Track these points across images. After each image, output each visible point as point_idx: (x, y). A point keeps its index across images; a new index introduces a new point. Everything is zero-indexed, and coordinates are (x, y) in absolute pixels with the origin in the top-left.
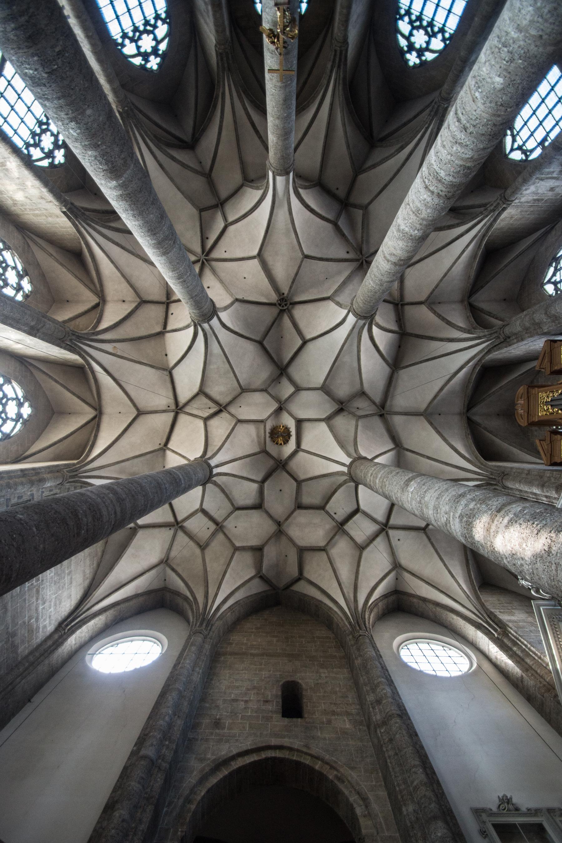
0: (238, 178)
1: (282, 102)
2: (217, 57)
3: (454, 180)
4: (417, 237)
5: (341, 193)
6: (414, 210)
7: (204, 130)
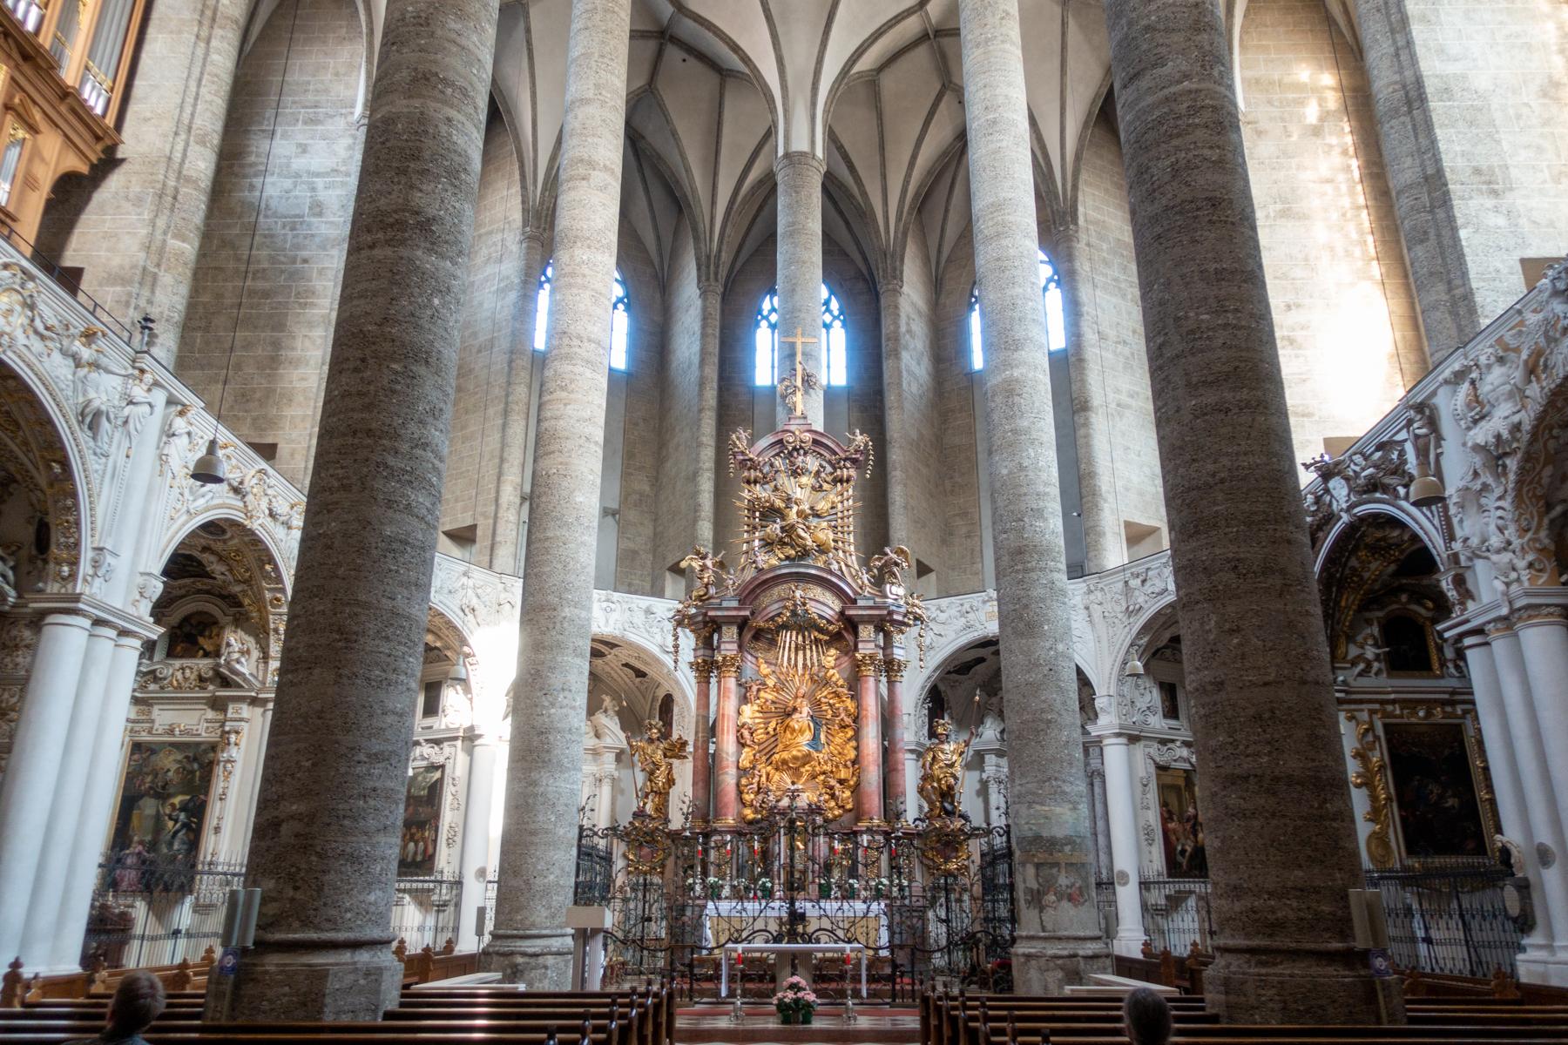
0: (888, 82)
1: (798, 289)
2: (902, 273)
3: (570, 367)
4: (579, 244)
5: (673, 54)
6: (602, 299)
7: (944, 154)
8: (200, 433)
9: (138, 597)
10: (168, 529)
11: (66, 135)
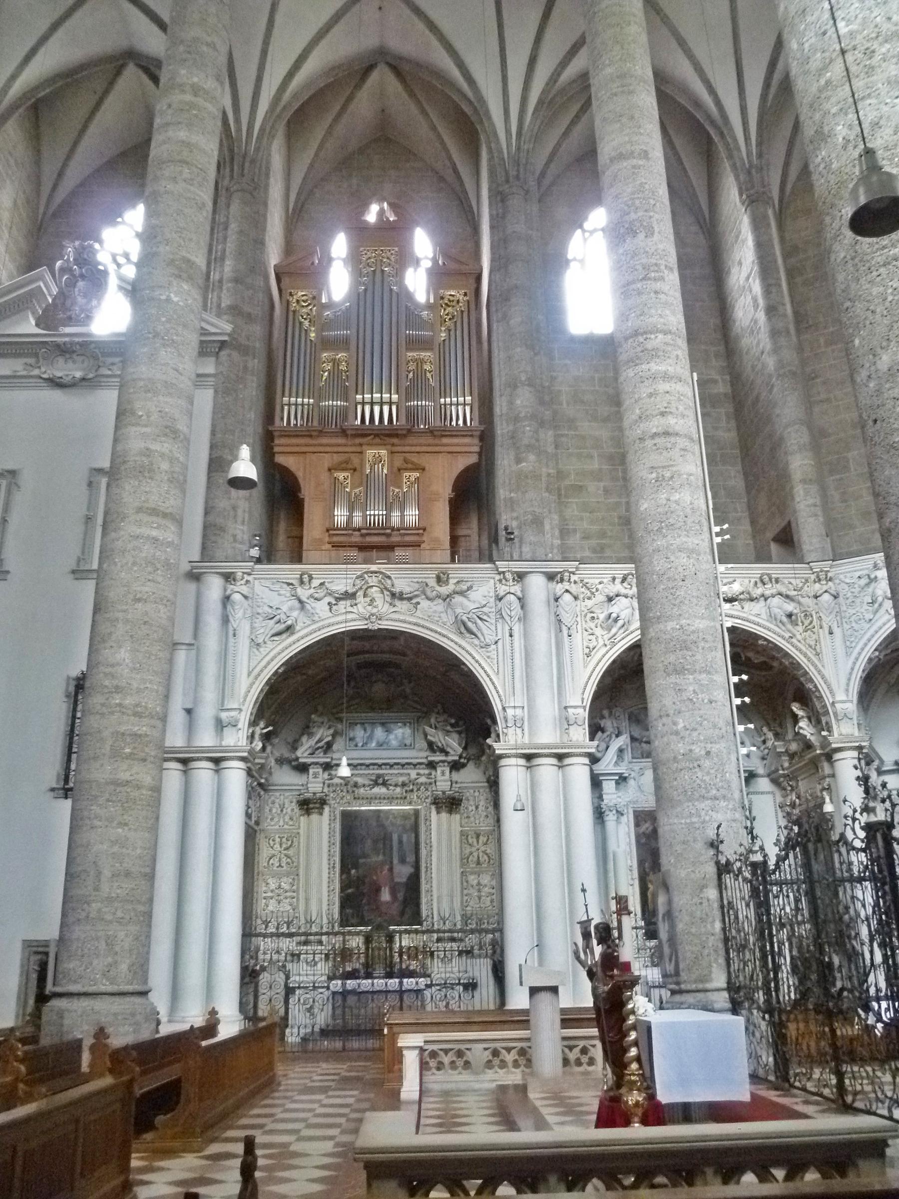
8: (597, 581)
9: (567, 727)
10: (585, 667)
11: (449, 452)
